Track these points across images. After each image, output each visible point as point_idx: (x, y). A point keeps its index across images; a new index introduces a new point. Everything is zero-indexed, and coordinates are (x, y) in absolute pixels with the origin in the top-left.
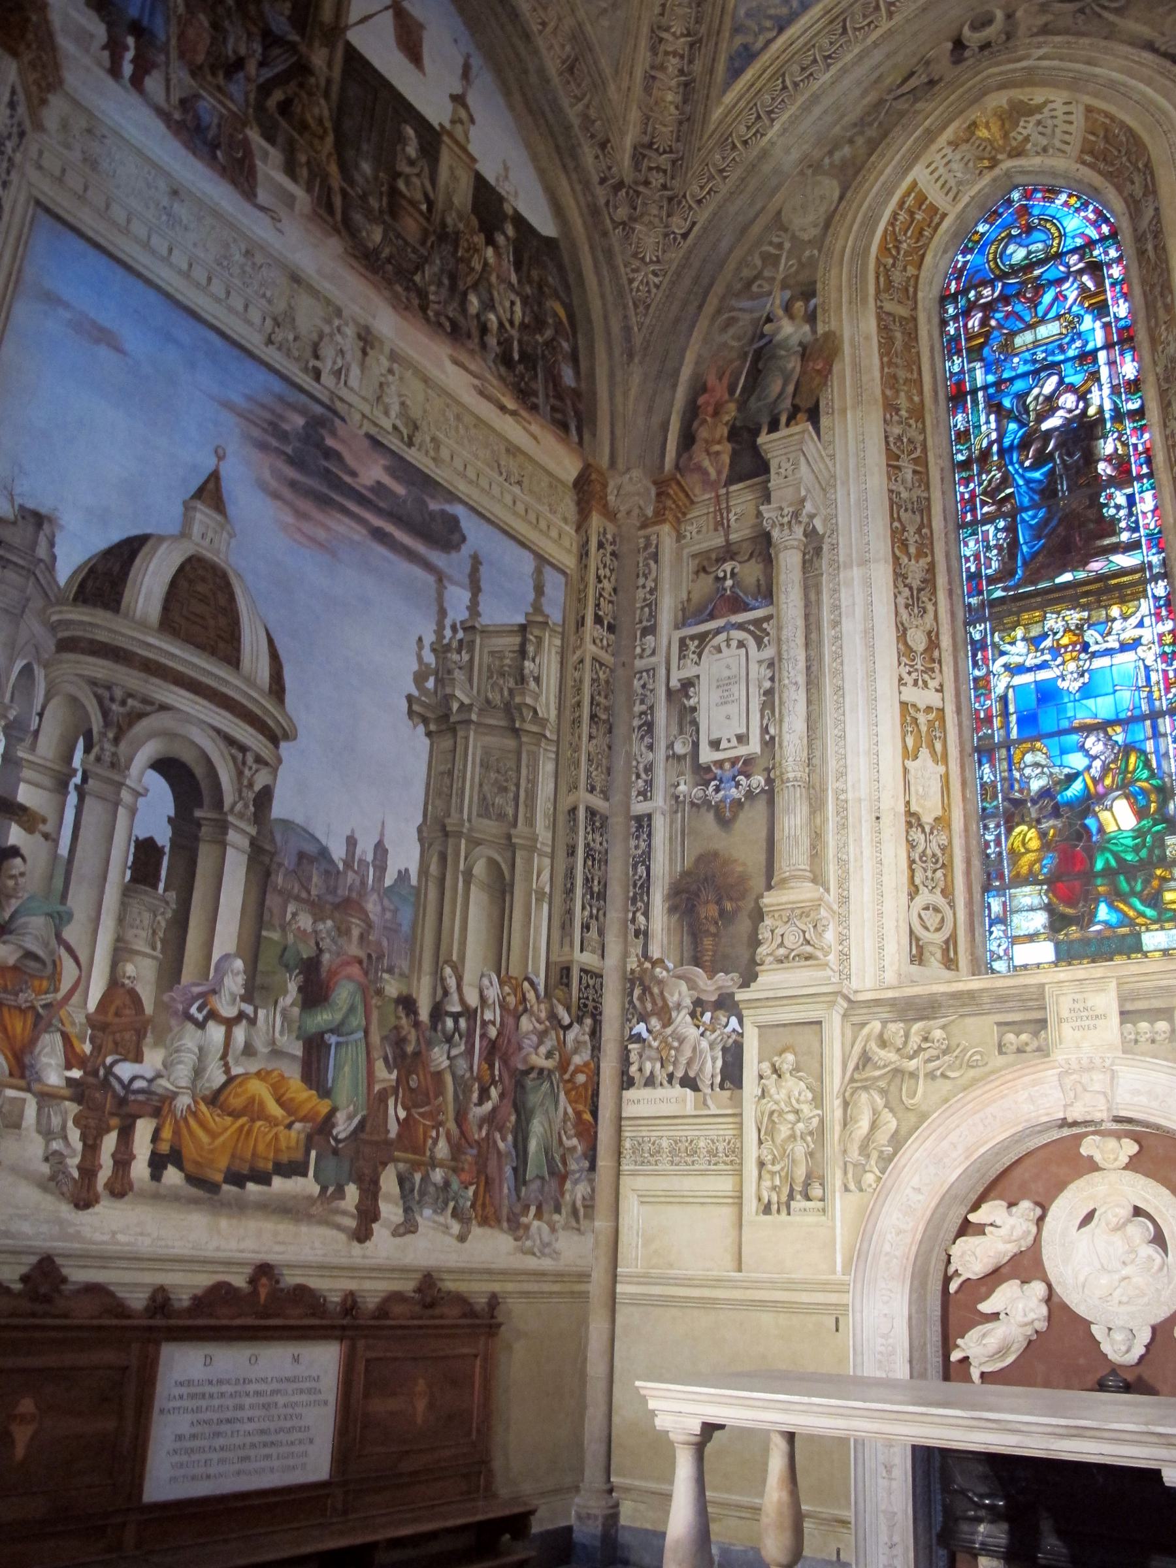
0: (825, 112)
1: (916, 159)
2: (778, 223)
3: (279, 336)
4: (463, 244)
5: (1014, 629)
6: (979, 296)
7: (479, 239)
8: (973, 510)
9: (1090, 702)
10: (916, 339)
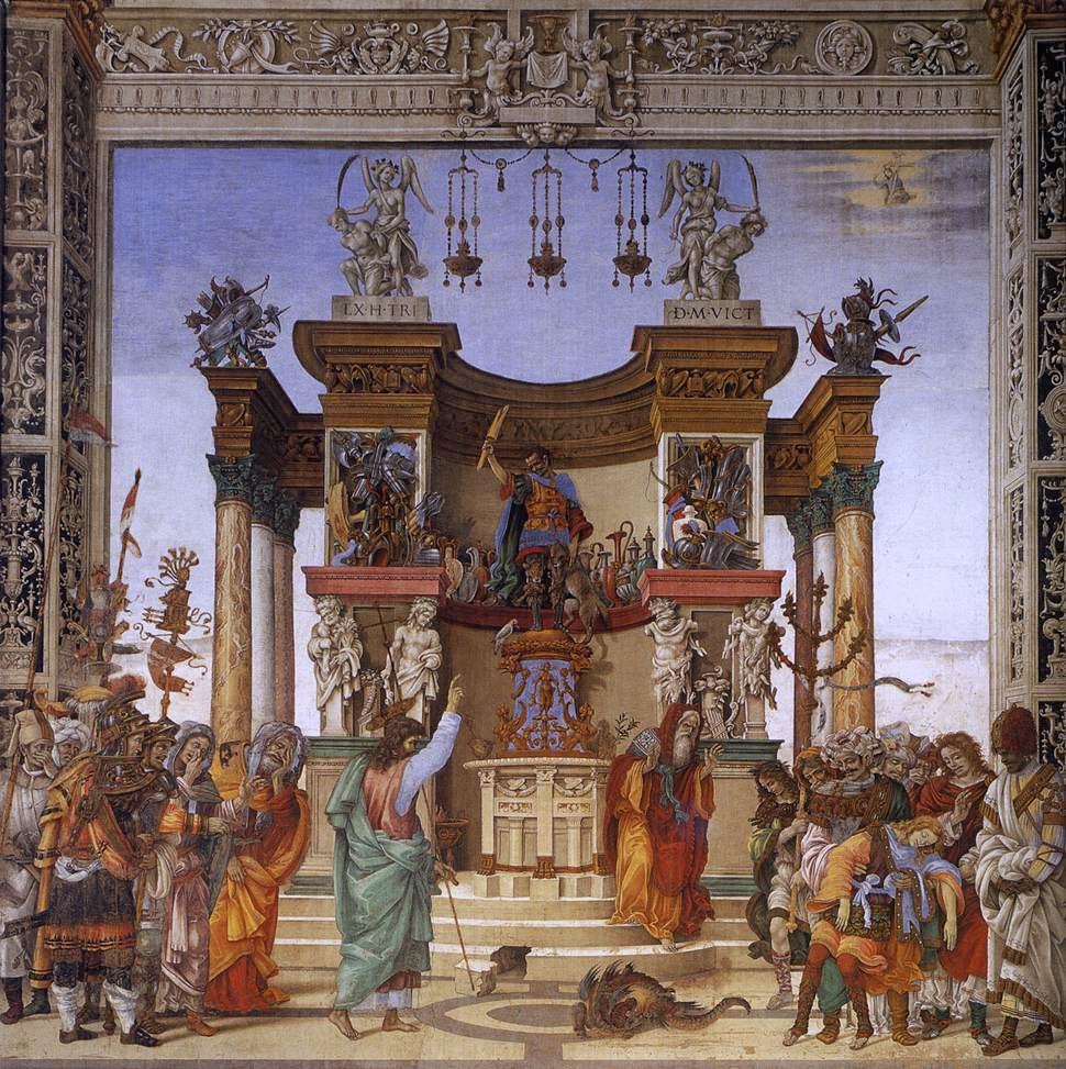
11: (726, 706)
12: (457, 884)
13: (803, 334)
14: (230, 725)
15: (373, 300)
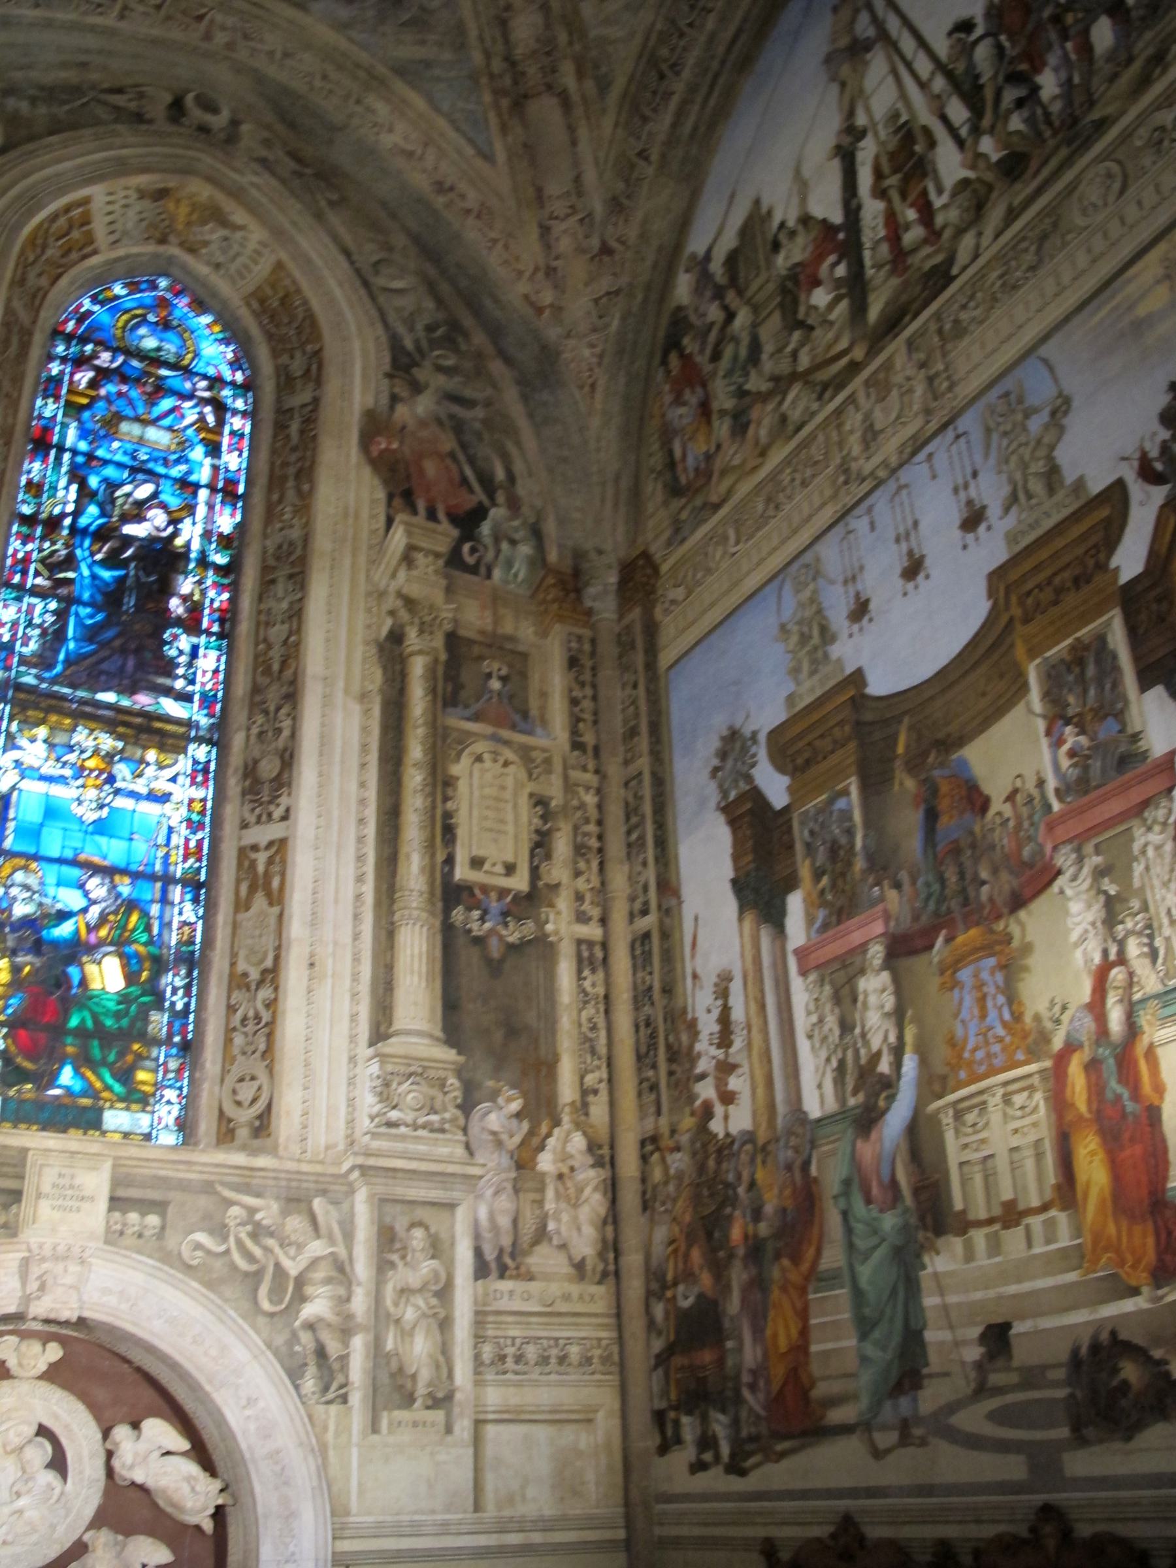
5: (37, 725)
6: (95, 355)
8: (24, 573)
9: (103, 840)
11: (1151, 945)
12: (938, 1253)
14: (764, 1125)
15: (808, 684)
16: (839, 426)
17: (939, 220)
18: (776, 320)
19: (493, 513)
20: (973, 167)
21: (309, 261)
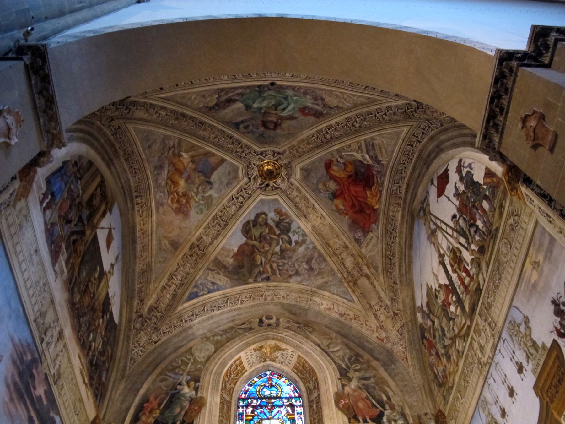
0: (214, 323)
1: (242, 350)
2: (190, 350)
3: (38, 320)
4: (96, 314)
6: (252, 402)
7: (100, 314)
10: (230, 410)
13: (556, 338)
16: (473, 349)
17: (471, 273)
18: (444, 319)
19: (386, 413)
20: (473, 255)
21: (307, 352)
